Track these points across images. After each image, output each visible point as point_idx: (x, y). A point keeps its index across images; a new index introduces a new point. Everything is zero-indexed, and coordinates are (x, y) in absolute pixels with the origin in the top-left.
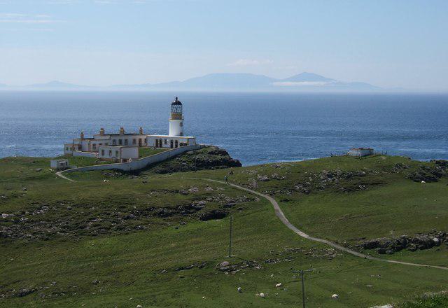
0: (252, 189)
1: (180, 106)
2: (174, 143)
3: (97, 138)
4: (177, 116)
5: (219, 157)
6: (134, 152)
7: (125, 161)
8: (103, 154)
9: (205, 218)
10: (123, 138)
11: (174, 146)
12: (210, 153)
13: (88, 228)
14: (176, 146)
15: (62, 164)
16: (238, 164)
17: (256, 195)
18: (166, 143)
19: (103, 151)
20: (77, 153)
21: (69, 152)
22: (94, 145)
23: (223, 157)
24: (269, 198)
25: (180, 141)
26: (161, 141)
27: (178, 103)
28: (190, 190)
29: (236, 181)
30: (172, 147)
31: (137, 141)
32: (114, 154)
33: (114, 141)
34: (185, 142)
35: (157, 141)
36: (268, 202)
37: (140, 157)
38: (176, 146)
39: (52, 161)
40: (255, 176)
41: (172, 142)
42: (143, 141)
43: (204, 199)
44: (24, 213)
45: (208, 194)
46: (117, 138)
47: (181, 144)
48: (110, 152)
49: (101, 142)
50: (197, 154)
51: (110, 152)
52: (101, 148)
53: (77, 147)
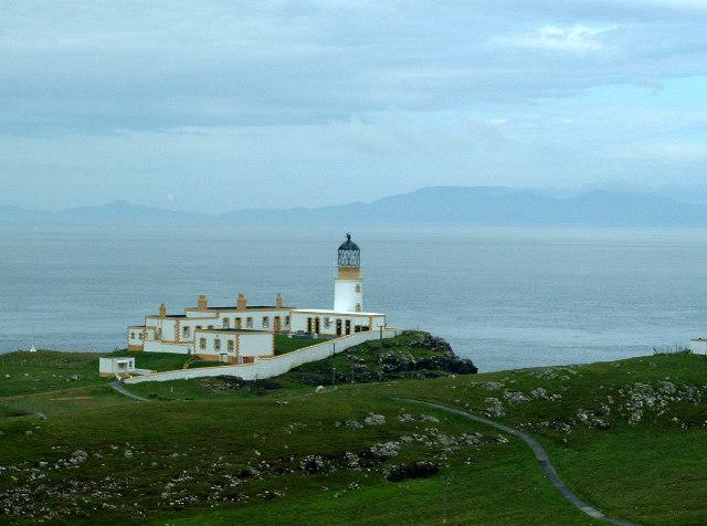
0: (493, 419)
2: (343, 327)
3: (189, 314)
4: (348, 270)
5: (432, 355)
6: (266, 343)
7: (248, 360)
8: (203, 346)
9: (396, 477)
10: (244, 315)
11: (343, 332)
13: (165, 495)
14: (348, 332)
15: (122, 365)
16: (467, 368)
17: (502, 432)
18: (327, 323)
19: (203, 340)
20: (151, 347)
21: (136, 342)
22: (186, 328)
23: (440, 355)
24: (525, 437)
25: (355, 322)
26: (317, 320)
27: (348, 246)
28: (368, 420)
29: (462, 405)
30: (339, 331)
31: (271, 322)
32: (224, 348)
33: (226, 320)
34: (365, 323)
35: (310, 319)
36: (524, 447)
37: (277, 353)
38: (348, 332)
39: (102, 360)
40: (498, 394)
41: (339, 323)
42: (283, 321)
43: (397, 439)
44: (37, 465)
45: (408, 428)
46: (232, 316)
47: (358, 329)
48: (217, 341)
49: (199, 323)
51: (217, 341)
52: (200, 335)
53: (151, 333)
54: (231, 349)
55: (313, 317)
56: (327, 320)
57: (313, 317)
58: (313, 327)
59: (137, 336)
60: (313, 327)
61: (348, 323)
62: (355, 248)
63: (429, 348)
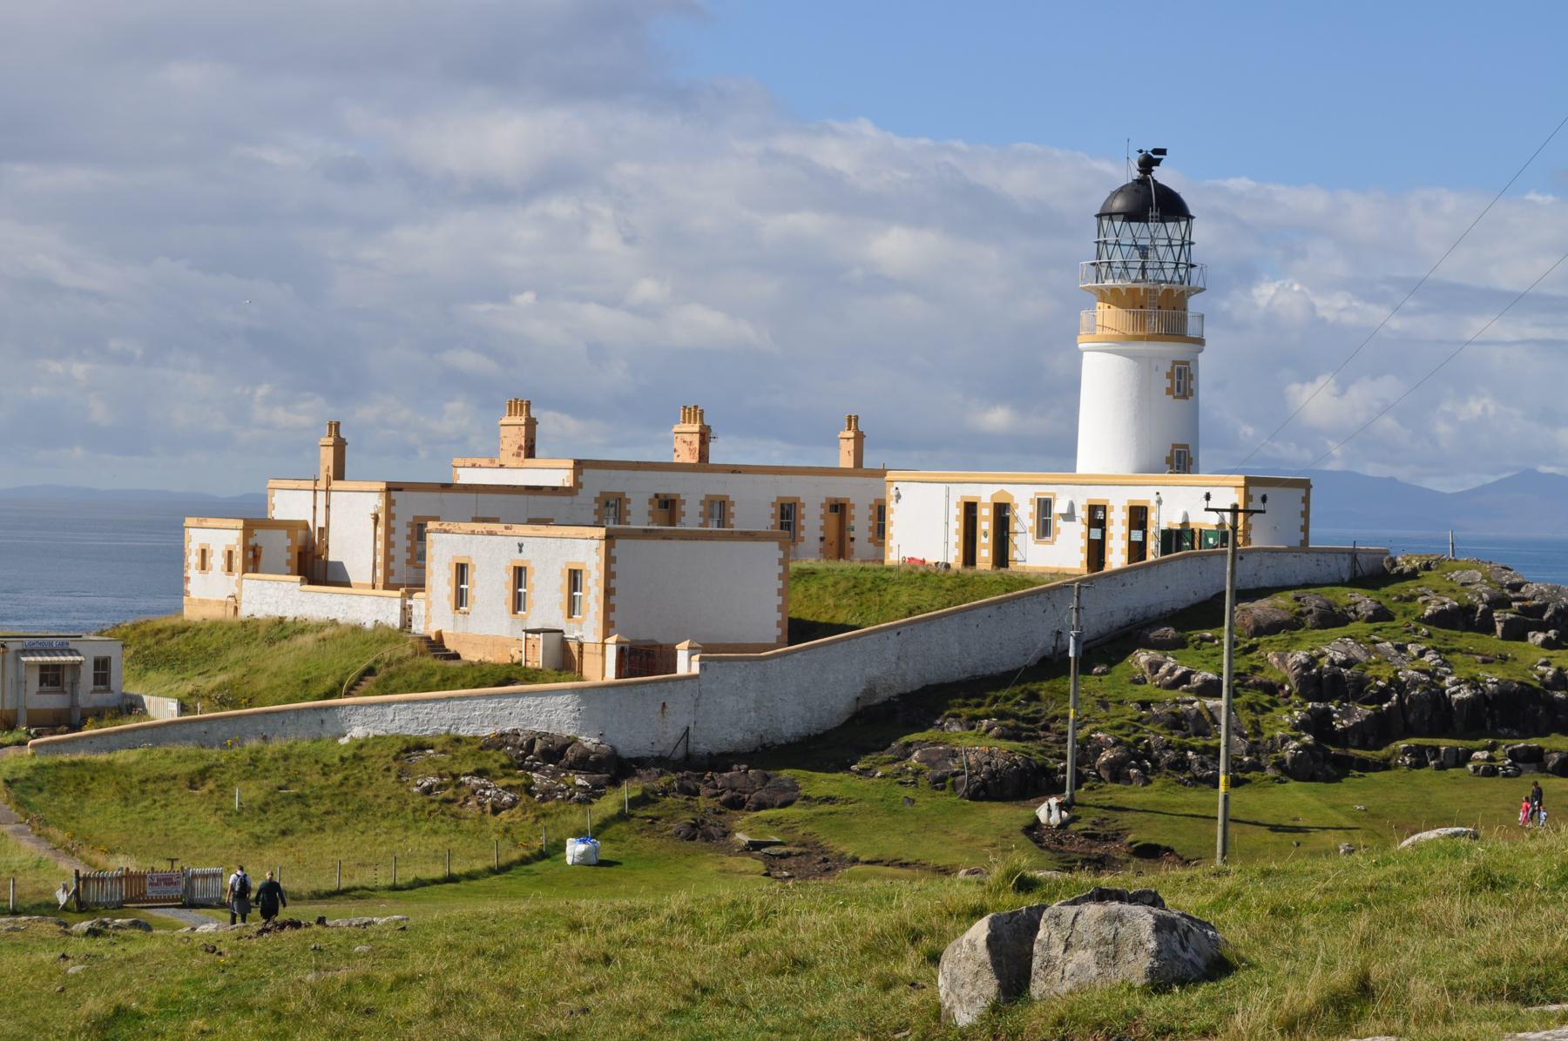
1: (1174, 229)
11: (1116, 557)
12: (1442, 619)
14: (1137, 550)
18: (1044, 529)
19: (461, 570)
20: (277, 596)
26: (1002, 513)
30: (1096, 552)
32: (546, 607)
35: (970, 509)
41: (1097, 517)
42: (860, 524)
48: (519, 574)
50: (1332, 618)
51: (519, 574)
53: (279, 546)
54: (572, 607)
55: (985, 496)
56: (1044, 506)
57: (985, 496)
58: (985, 553)
59: (217, 561)
60: (985, 553)
61: (1138, 517)
62: (1171, 207)
63: (1516, 632)
